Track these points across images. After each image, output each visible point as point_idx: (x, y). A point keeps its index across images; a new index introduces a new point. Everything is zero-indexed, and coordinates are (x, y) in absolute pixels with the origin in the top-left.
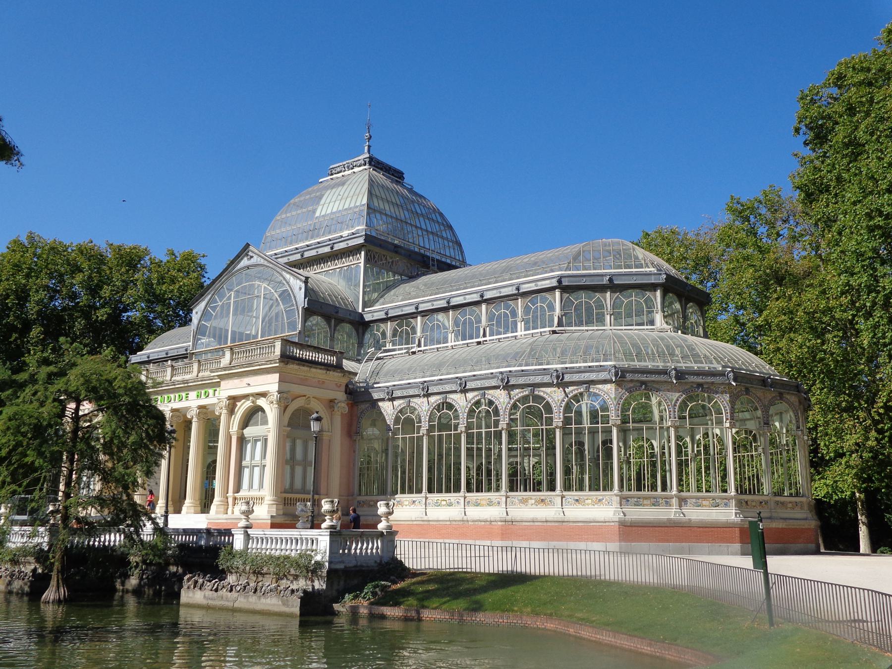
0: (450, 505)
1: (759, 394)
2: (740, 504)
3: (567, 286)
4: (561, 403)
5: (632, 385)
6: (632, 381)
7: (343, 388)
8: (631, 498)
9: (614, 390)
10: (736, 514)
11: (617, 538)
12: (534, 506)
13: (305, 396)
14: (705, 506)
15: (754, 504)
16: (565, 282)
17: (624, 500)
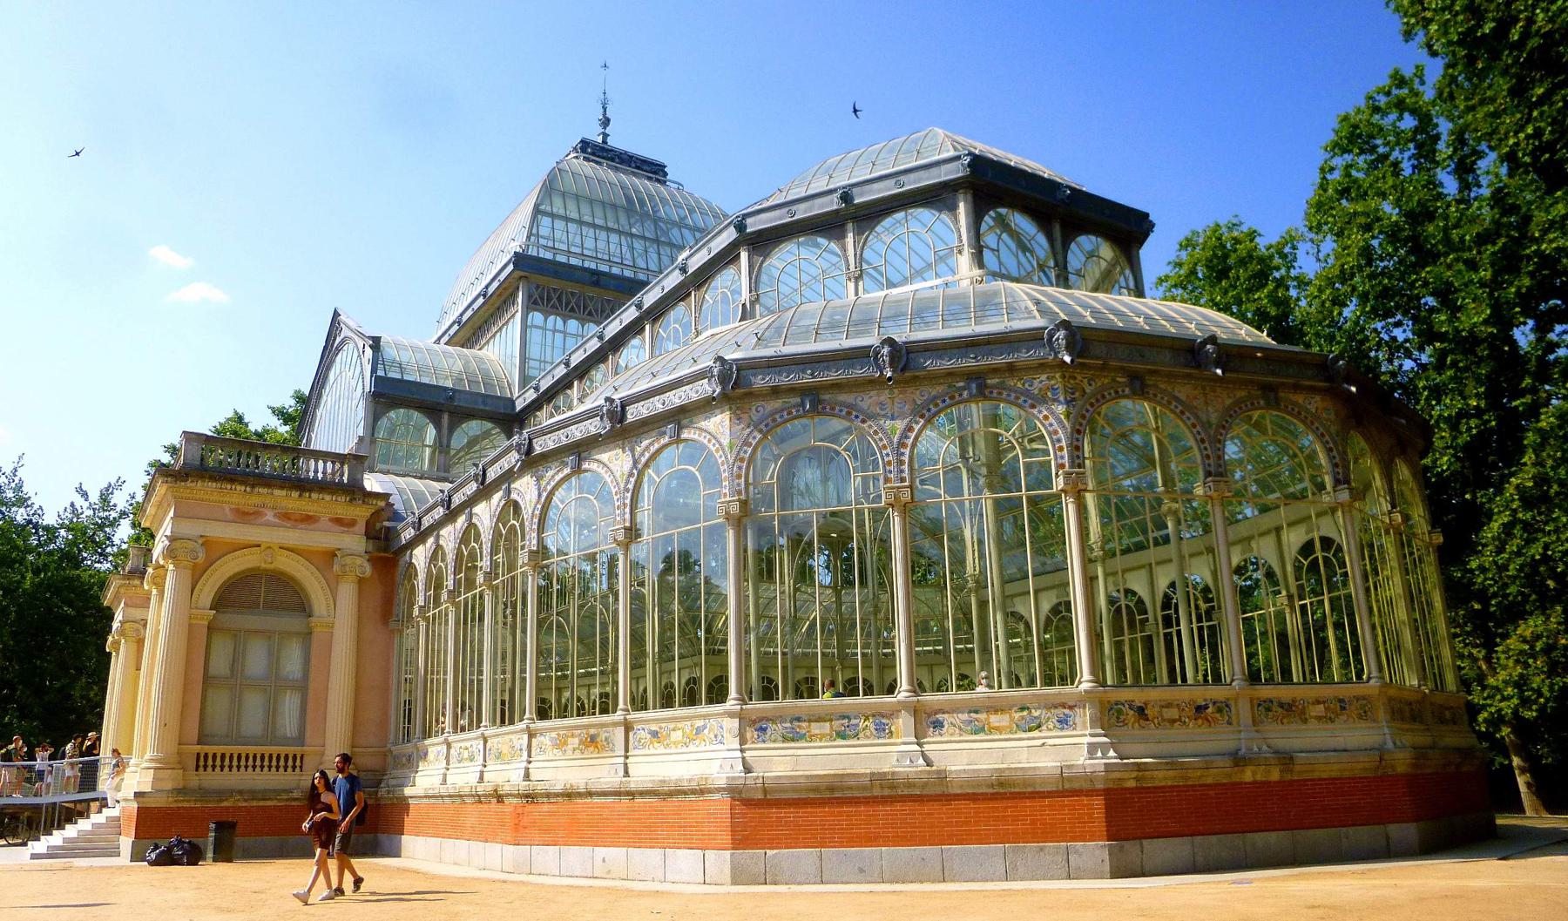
0: (471, 759)
1: (1183, 391)
2: (1110, 716)
3: (760, 233)
4: (627, 482)
5: (777, 404)
6: (776, 392)
7: (361, 527)
8: (772, 720)
9: (727, 422)
10: (1092, 748)
11: (726, 838)
12: (578, 754)
13: (259, 546)
14: (999, 730)
15: (1173, 713)
16: (753, 225)
17: (753, 727)
